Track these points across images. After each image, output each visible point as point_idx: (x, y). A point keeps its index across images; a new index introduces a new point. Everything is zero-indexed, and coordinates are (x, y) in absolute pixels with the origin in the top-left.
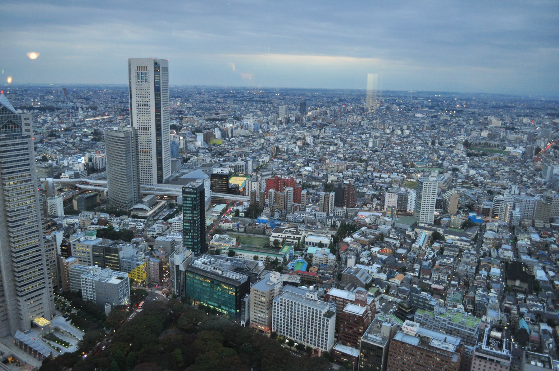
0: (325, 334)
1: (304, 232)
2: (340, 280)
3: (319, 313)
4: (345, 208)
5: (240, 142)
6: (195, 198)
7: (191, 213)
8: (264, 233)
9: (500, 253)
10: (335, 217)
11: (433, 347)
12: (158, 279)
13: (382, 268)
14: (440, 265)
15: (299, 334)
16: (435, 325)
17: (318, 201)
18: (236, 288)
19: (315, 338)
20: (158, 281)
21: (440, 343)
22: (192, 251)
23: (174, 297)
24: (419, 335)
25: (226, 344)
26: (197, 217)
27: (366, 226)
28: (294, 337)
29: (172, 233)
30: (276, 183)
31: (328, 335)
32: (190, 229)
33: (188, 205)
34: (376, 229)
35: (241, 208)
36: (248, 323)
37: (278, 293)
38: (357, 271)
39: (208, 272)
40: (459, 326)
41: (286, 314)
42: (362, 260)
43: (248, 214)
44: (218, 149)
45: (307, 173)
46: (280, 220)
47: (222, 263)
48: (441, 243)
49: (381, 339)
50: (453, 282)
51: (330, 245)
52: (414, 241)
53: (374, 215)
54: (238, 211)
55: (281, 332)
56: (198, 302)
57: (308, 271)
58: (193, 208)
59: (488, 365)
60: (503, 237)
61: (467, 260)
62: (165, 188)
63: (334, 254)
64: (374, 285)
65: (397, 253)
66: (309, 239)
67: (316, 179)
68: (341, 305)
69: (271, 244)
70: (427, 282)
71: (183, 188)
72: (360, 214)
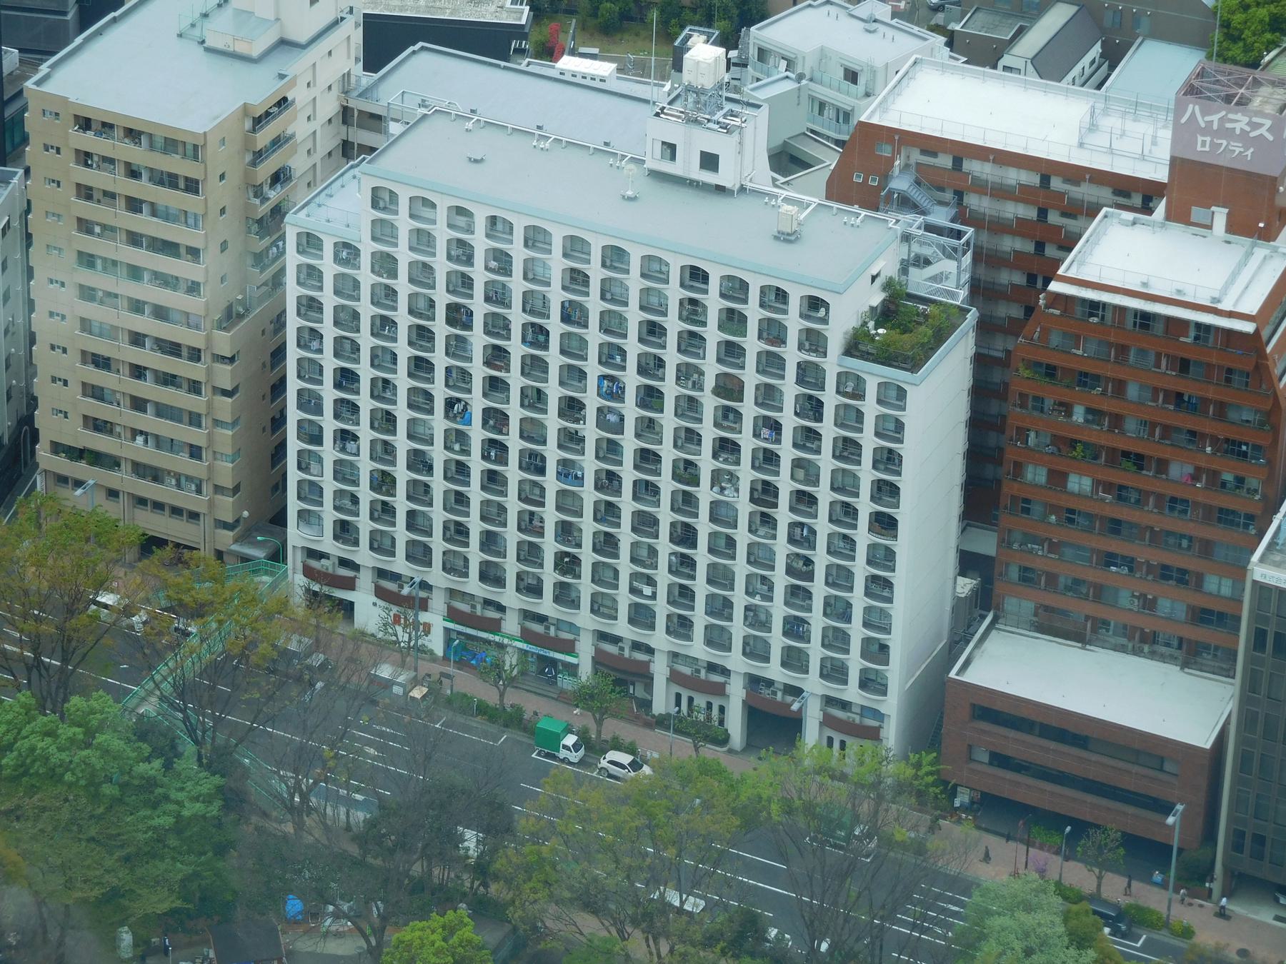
37: (328, 141)
41: (440, 360)
68: (1019, 228)
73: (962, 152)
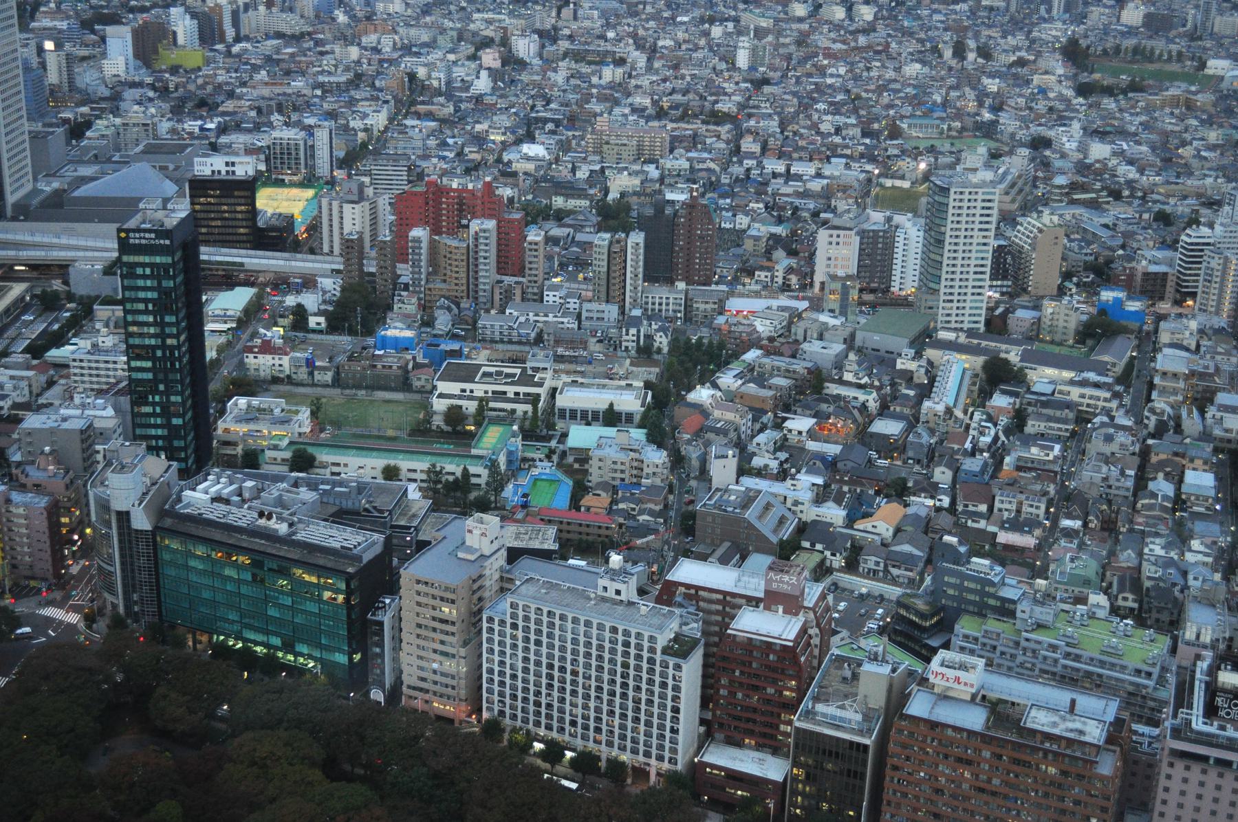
0: (669, 714)
1: (548, 375)
2: (690, 533)
3: (646, 644)
4: (681, 285)
5: (269, 60)
6: (166, 267)
7: (155, 324)
8: (405, 384)
9: (1209, 421)
10: (649, 318)
11: (1034, 732)
12: (48, 566)
13: (826, 486)
14: (1019, 469)
15: (580, 721)
16: (1021, 665)
17: (581, 264)
18: (349, 578)
19: (634, 730)
20: (50, 575)
21: (1056, 719)
22: (169, 458)
23: (117, 623)
24: (984, 697)
25: (332, 769)
26: (177, 336)
27: (761, 348)
28: (561, 730)
29: (77, 399)
30: (429, 205)
31: (681, 716)
32: (155, 381)
33: (142, 295)
34: (794, 356)
35: (310, 301)
36: (394, 694)
37: (496, 588)
38: (748, 499)
39: (239, 530)
40: (1102, 664)
41: (532, 657)
42: (757, 462)
43: (338, 320)
44: (191, 87)
45: (530, 167)
46: (455, 337)
47: (286, 496)
48: (1016, 395)
49: (859, 717)
50: (1066, 523)
51: (645, 416)
52: (926, 391)
53: (782, 309)
54: (300, 314)
55: (514, 717)
56: (204, 638)
57: (578, 509)
58: (162, 306)
59: (1212, 777)
60: (1217, 369)
61: (1107, 449)
62: (19, 238)
63: (660, 446)
64: (806, 544)
65: (873, 435)
66: (570, 399)
67: (569, 189)
68: (717, 613)
69: (438, 421)
70: (982, 524)
71: (119, 230)
72: (734, 304)
73: (698, 588)
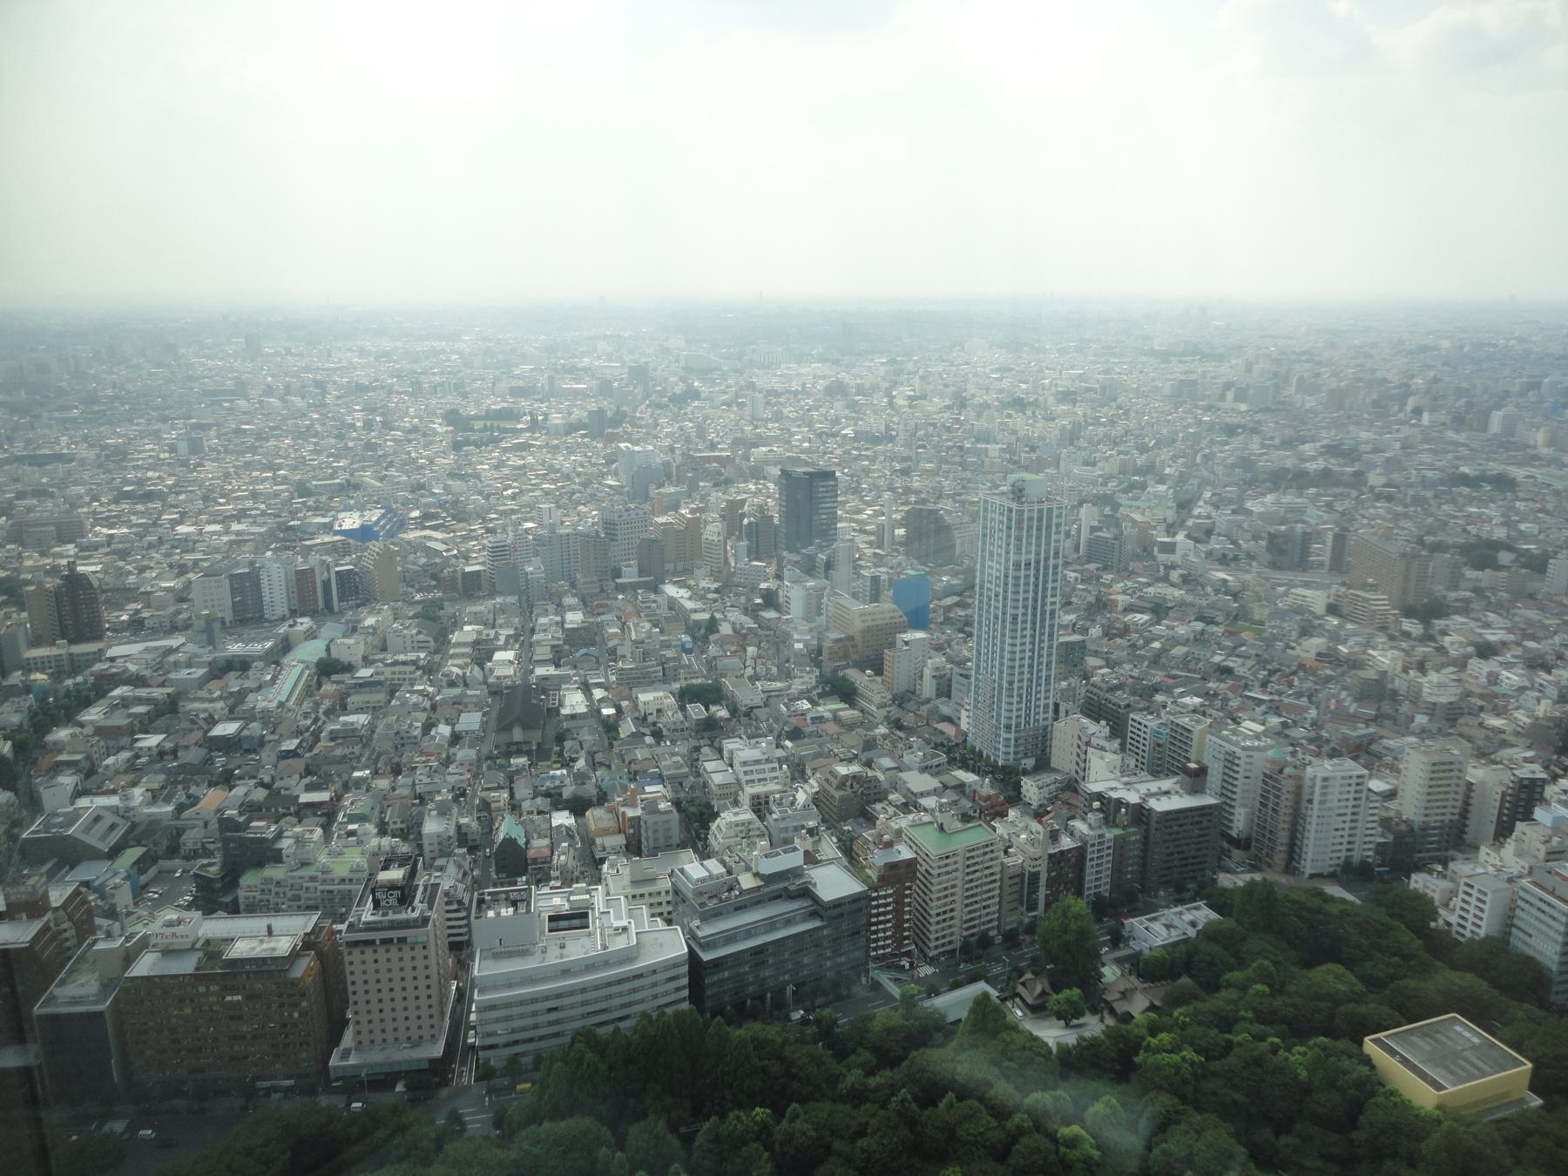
59: (382, 954)
